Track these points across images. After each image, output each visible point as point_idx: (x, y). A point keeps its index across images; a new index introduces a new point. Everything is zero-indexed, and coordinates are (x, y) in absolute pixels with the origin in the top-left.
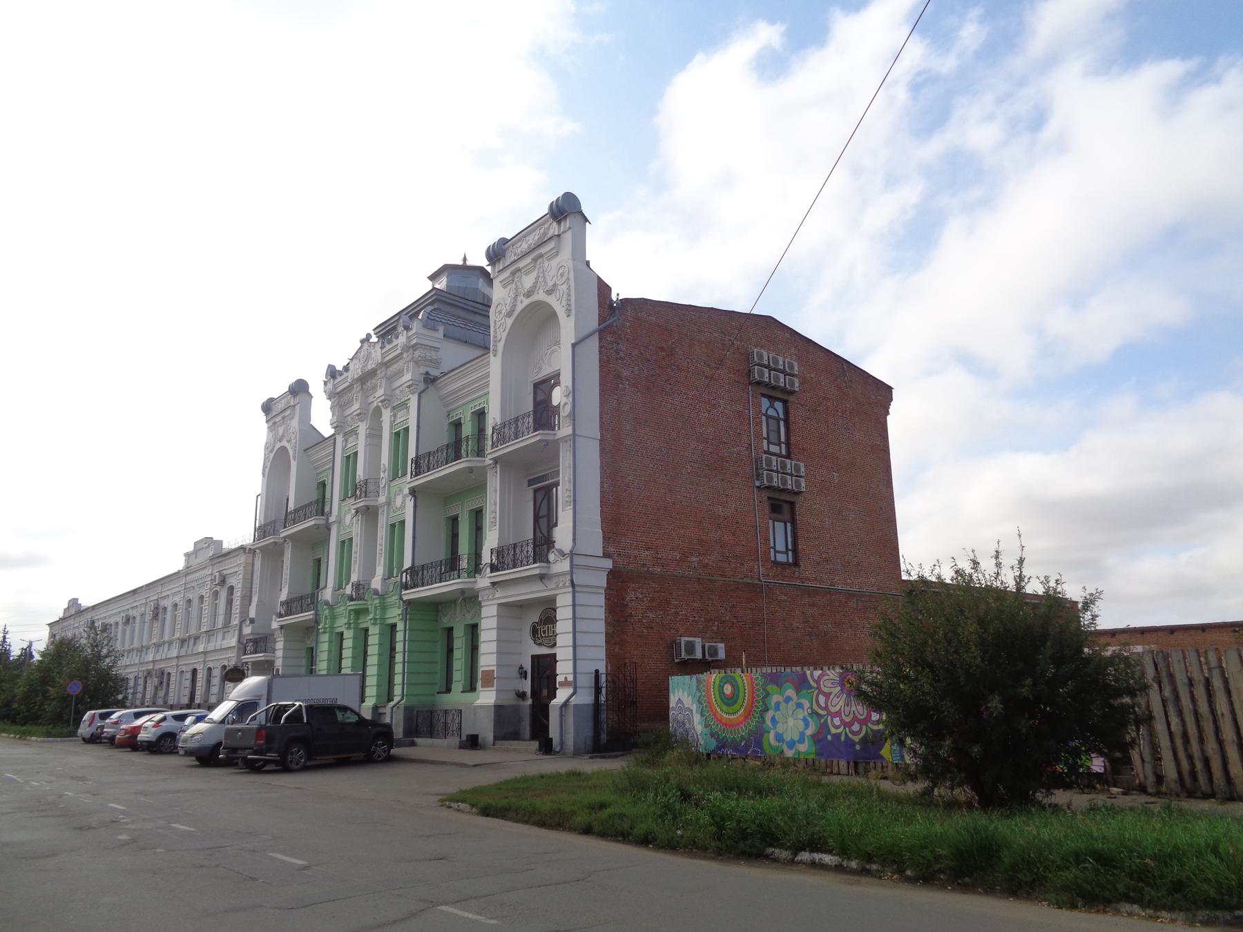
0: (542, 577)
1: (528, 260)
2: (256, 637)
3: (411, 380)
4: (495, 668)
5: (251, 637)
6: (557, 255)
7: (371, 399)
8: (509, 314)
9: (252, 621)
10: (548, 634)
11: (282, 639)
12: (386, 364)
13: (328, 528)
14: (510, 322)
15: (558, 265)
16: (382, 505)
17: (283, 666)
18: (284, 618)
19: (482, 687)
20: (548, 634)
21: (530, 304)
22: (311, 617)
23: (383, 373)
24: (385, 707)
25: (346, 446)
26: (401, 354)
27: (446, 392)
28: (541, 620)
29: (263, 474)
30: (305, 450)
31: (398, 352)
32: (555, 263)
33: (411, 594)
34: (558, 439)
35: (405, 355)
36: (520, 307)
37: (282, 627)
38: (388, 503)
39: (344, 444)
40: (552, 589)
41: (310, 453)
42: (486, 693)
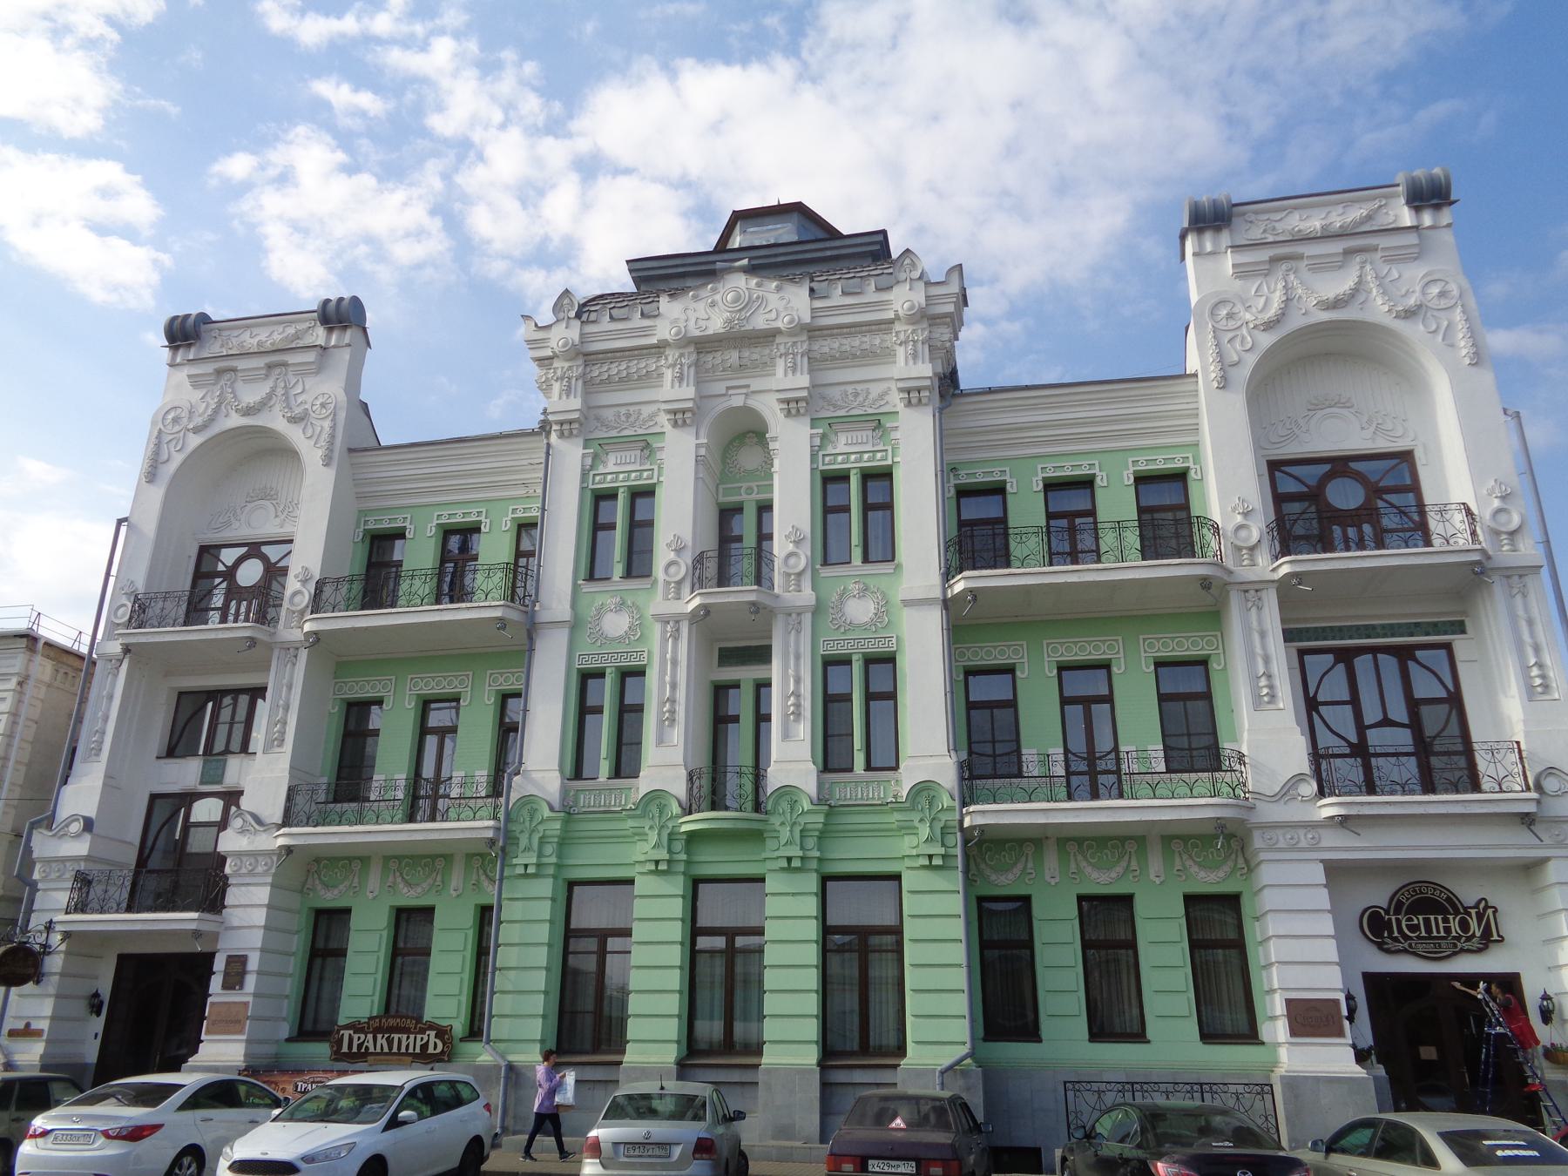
0: (1527, 820)
1: (1336, 247)
2: (91, 866)
3: (930, 378)
4: (1341, 997)
5: (82, 866)
6: (1416, 259)
7: (719, 388)
8: (1269, 326)
9: (88, 825)
10: (1428, 929)
11: (269, 880)
12: (812, 331)
13: (532, 630)
14: (1267, 340)
15: (1423, 278)
16: (793, 614)
17: (263, 950)
18: (319, 829)
19: (1294, 1033)
20: (1428, 929)
21: (1331, 322)
22: (490, 834)
23: (805, 346)
24: (895, 1067)
25: (592, 467)
26: (891, 322)
27: (972, 424)
28: (1399, 905)
29: (151, 475)
30: (351, 450)
31: (891, 315)
32: (1414, 273)
33: (981, 815)
34: (1492, 569)
35: (898, 327)
36: (1296, 322)
37: (289, 850)
38: (818, 610)
39: (589, 461)
40: (1548, 847)
41: (364, 460)
42: (1305, 1048)
